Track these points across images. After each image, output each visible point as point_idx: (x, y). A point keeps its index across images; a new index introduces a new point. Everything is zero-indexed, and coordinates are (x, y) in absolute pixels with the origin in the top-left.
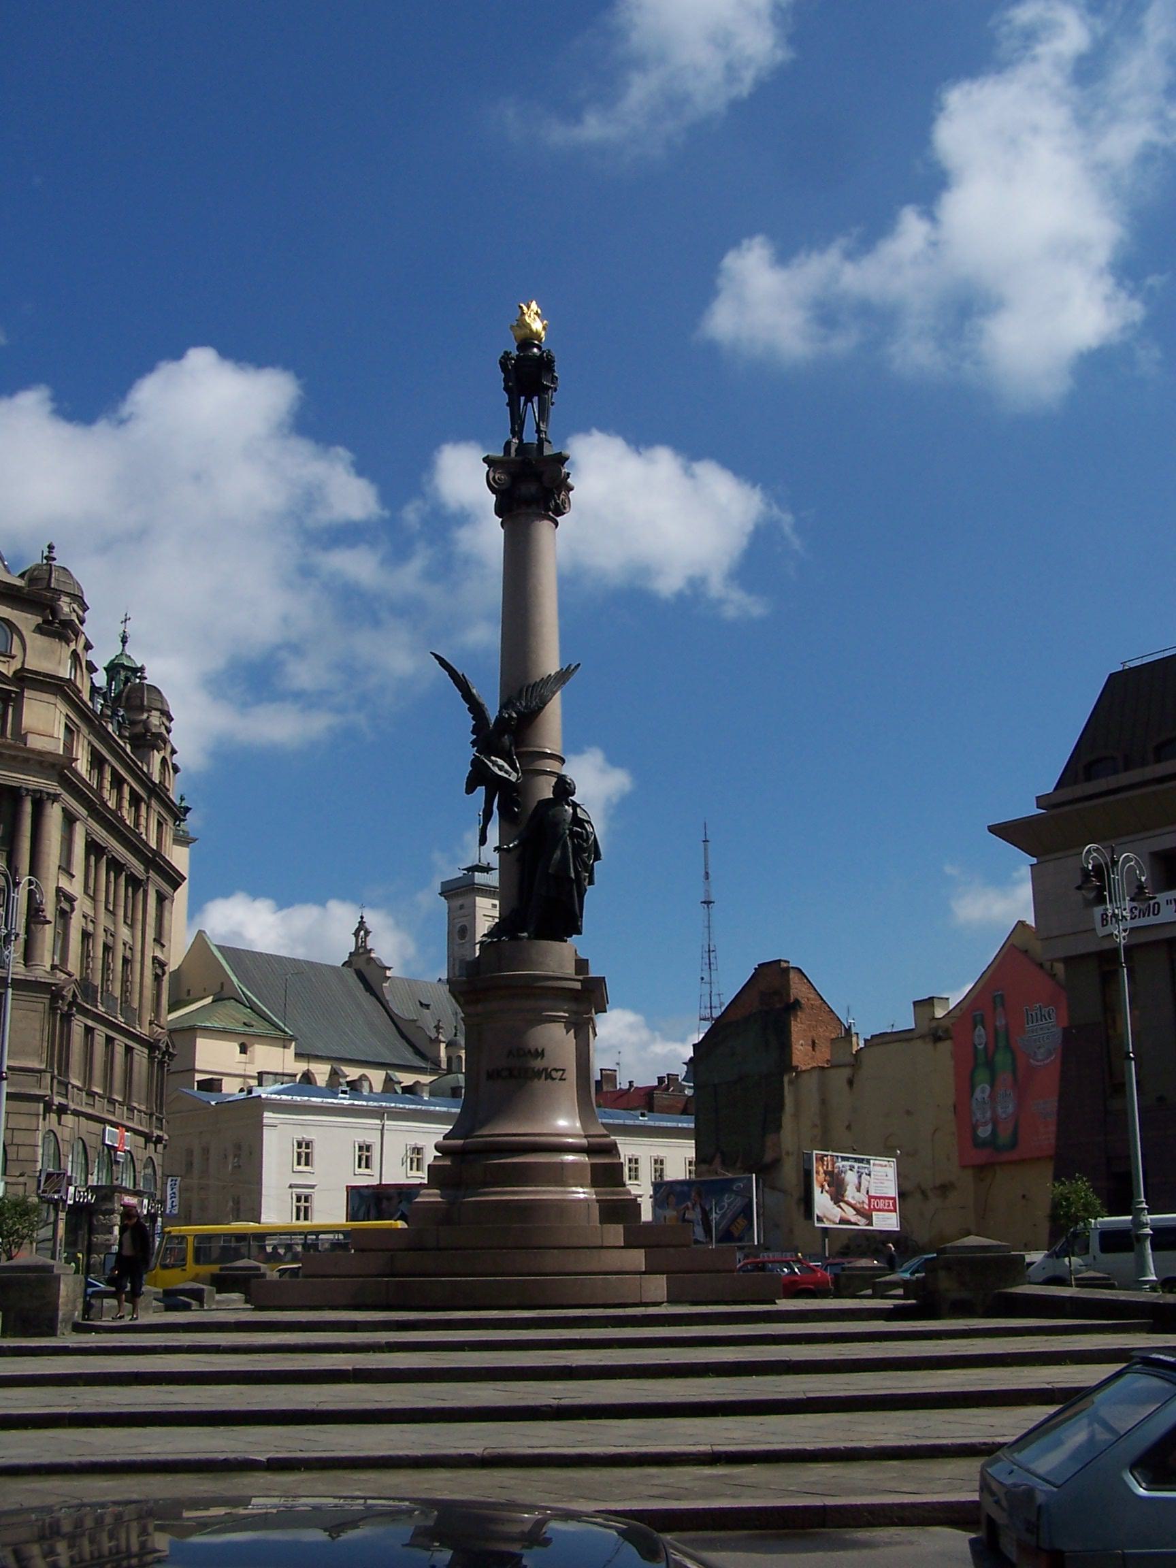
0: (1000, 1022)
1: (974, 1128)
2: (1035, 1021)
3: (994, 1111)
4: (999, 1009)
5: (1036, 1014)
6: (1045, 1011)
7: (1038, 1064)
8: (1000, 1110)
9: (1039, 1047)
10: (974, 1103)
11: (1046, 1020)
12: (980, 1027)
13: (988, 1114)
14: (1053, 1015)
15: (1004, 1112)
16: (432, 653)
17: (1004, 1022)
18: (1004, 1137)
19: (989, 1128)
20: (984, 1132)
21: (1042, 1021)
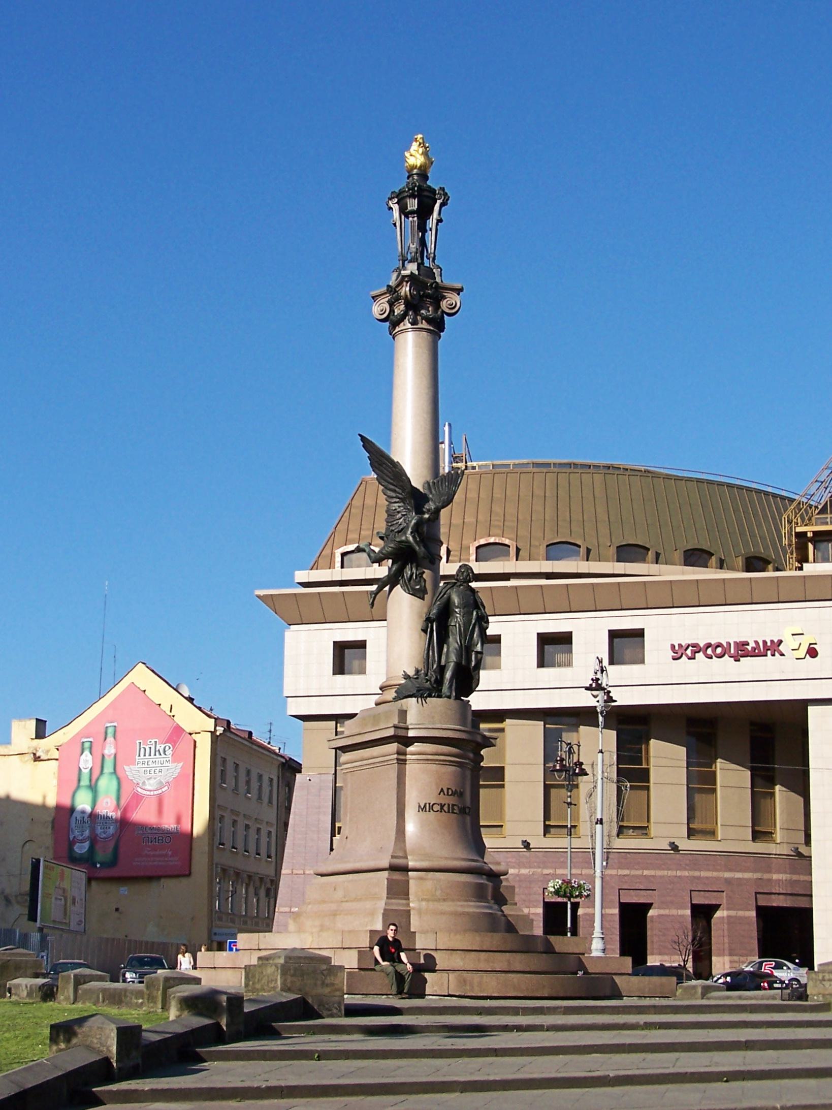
0: (109, 750)
1: (72, 844)
2: (147, 754)
3: (93, 830)
4: (110, 739)
5: (150, 748)
6: (160, 747)
7: (145, 792)
8: (99, 830)
9: (149, 779)
10: (73, 820)
11: (160, 755)
12: (87, 752)
13: (87, 833)
14: (169, 752)
15: (105, 833)
16: (360, 435)
17: (113, 751)
18: (102, 855)
19: (87, 845)
20: (81, 848)
21: (155, 755)
